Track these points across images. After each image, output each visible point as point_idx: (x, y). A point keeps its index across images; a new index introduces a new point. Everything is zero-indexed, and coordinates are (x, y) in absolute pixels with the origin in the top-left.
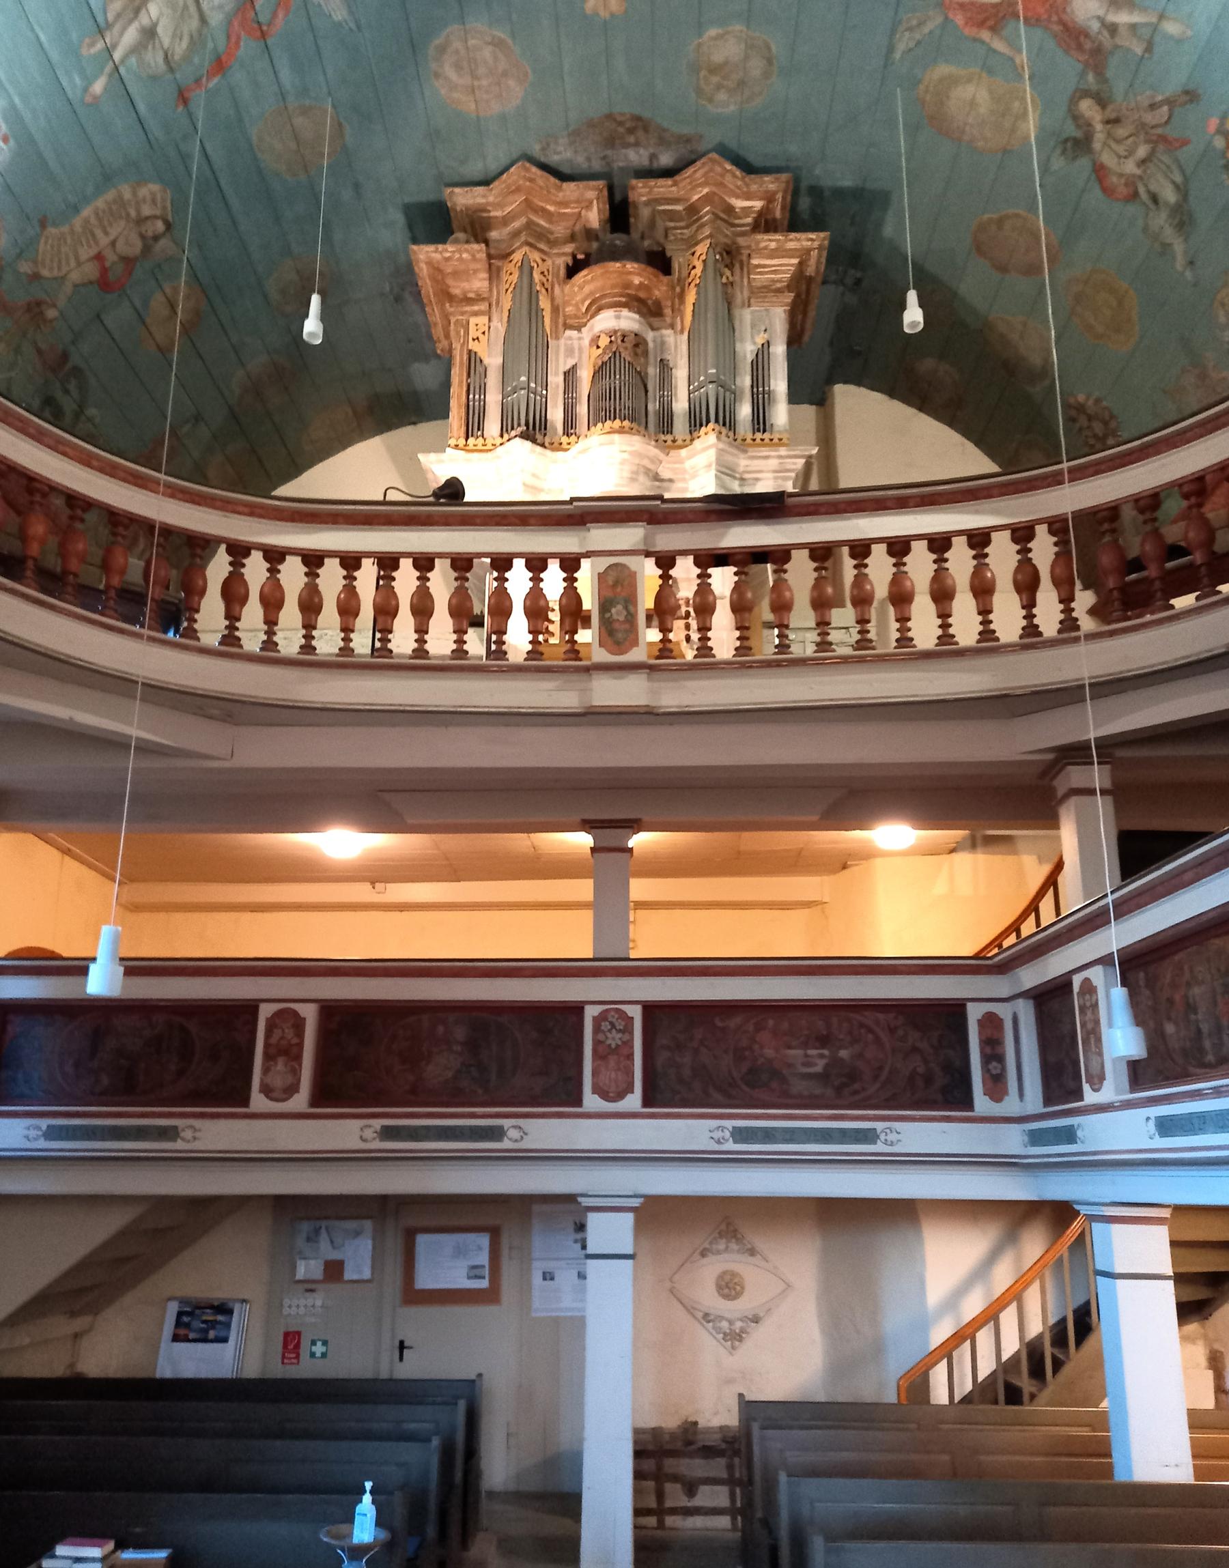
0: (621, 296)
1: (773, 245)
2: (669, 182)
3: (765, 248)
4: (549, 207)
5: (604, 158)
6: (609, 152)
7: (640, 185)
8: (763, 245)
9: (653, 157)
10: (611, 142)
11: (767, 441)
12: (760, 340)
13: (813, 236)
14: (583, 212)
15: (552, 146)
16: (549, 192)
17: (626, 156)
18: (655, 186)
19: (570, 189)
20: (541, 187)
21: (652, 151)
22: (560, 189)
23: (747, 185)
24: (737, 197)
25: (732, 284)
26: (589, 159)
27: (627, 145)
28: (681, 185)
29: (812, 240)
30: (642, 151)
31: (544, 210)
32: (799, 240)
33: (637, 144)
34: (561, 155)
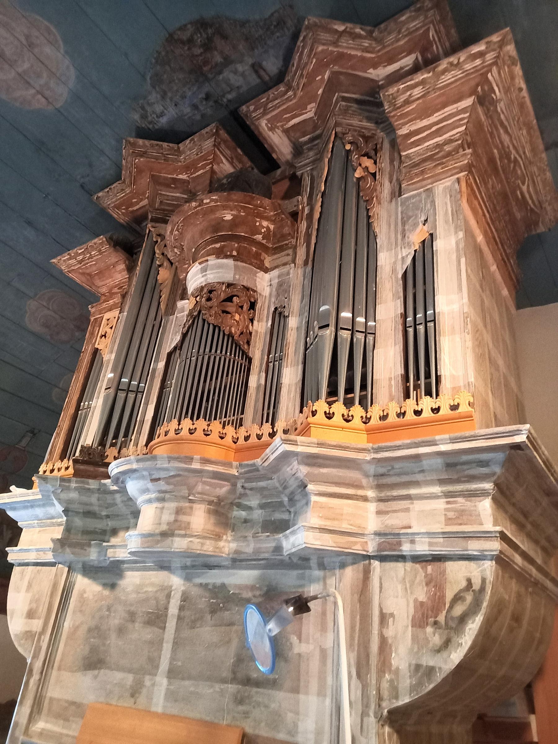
0: (216, 242)
1: (417, 92)
2: (282, 88)
3: (407, 102)
4: (180, 176)
5: (208, 97)
6: (206, 88)
7: (252, 108)
8: (402, 98)
9: (256, 68)
10: (199, 73)
11: (427, 414)
12: (416, 237)
13: (480, 47)
14: (215, 167)
15: (149, 109)
16: (166, 160)
17: (227, 82)
18: (269, 101)
19: (189, 150)
20: (156, 158)
21: (250, 61)
22: (179, 152)
23: (379, 41)
24: (375, 67)
25: (374, 175)
26: (195, 107)
27: (219, 69)
28: (294, 84)
29: (481, 54)
30: (240, 68)
31: (175, 180)
32: (458, 65)
33: (228, 62)
34: (166, 114)
